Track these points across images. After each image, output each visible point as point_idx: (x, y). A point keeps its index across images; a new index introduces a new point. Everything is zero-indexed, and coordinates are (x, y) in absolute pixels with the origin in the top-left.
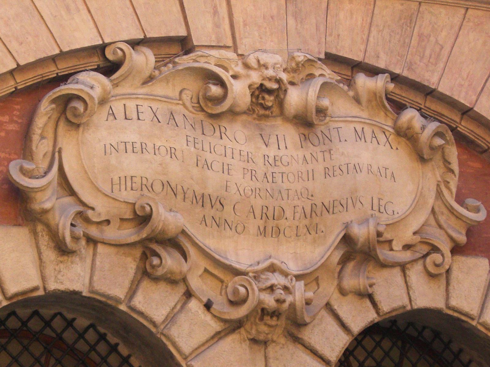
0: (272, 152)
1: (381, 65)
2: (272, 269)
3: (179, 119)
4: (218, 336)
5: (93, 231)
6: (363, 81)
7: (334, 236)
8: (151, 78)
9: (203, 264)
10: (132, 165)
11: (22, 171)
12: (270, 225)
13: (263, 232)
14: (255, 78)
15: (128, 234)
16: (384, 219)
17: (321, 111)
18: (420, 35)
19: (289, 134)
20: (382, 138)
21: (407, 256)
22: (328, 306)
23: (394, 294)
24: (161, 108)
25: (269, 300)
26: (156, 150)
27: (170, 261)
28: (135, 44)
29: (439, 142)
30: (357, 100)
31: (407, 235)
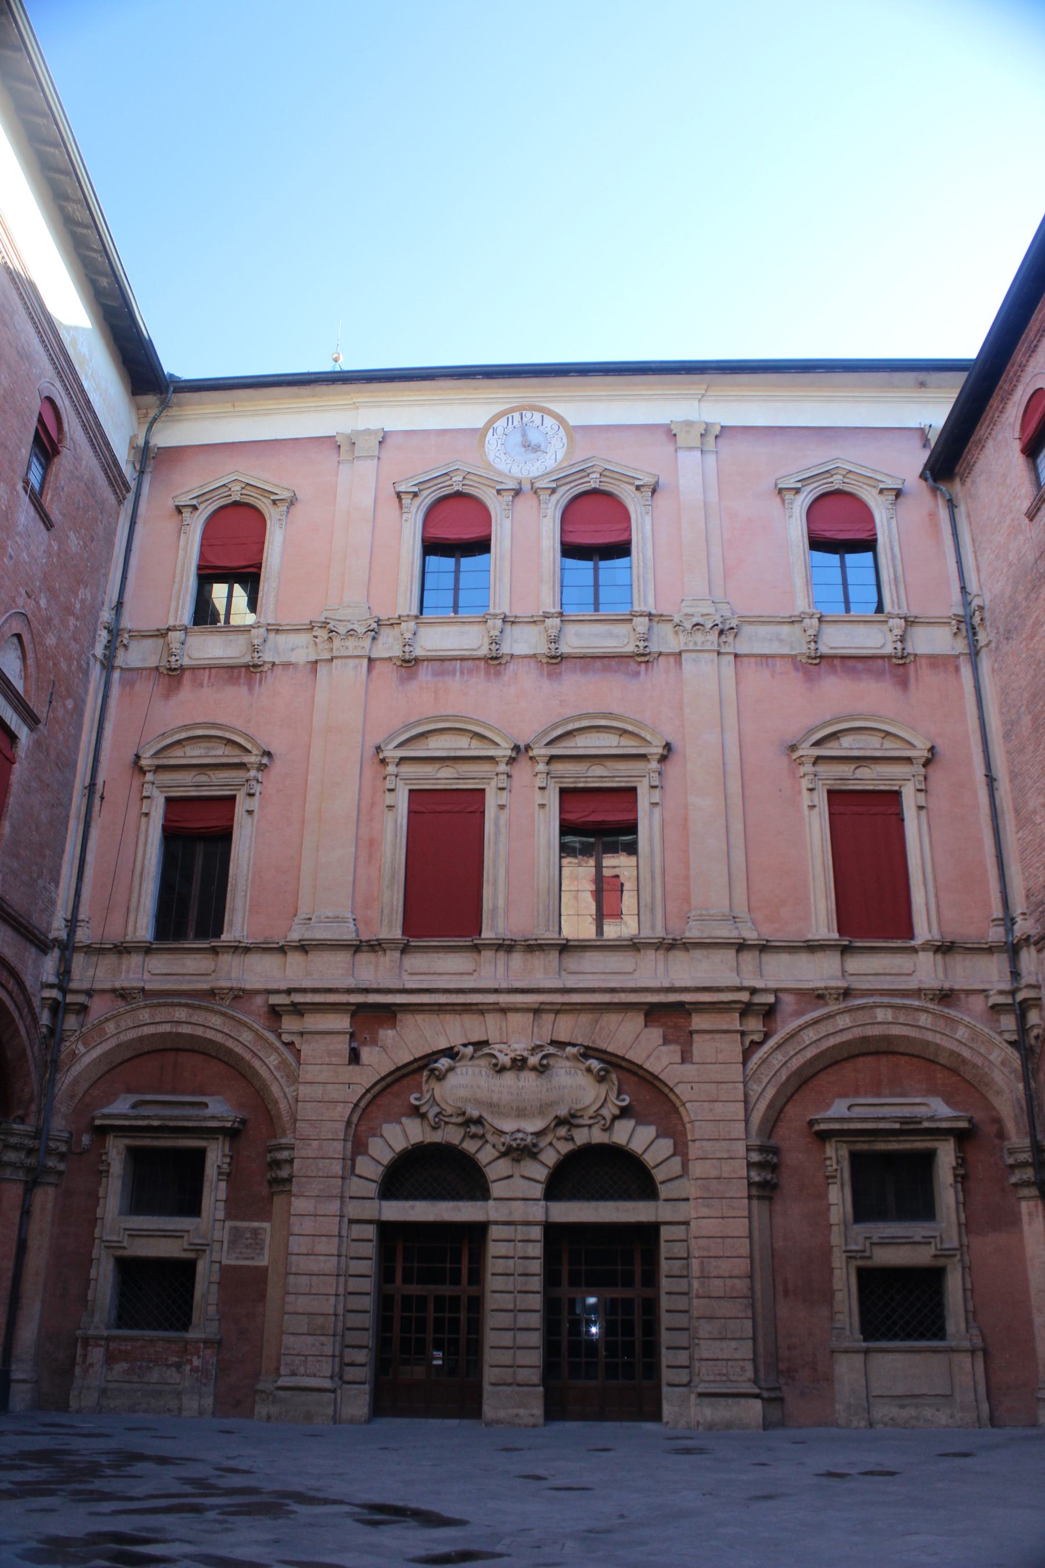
0: (521, 1084)
1: (579, 1042)
2: (519, 1131)
3: (484, 1073)
4: (498, 1158)
5: (447, 1119)
6: (569, 1050)
7: (551, 1117)
8: (472, 1058)
9: (492, 1130)
10: (462, 1093)
11: (416, 1099)
12: (521, 1113)
13: (518, 1116)
14: (512, 1055)
15: (460, 1120)
16: (579, 1107)
17: (541, 1065)
18: (601, 1028)
19: (532, 1075)
20: (580, 1073)
21: (591, 1121)
22: (551, 1144)
23: (581, 1137)
24: (477, 1070)
25: (514, 1144)
26: (472, 1087)
27: (473, 1129)
28: (465, 1045)
29: (602, 1073)
30: (567, 1058)
31: (591, 1112)
